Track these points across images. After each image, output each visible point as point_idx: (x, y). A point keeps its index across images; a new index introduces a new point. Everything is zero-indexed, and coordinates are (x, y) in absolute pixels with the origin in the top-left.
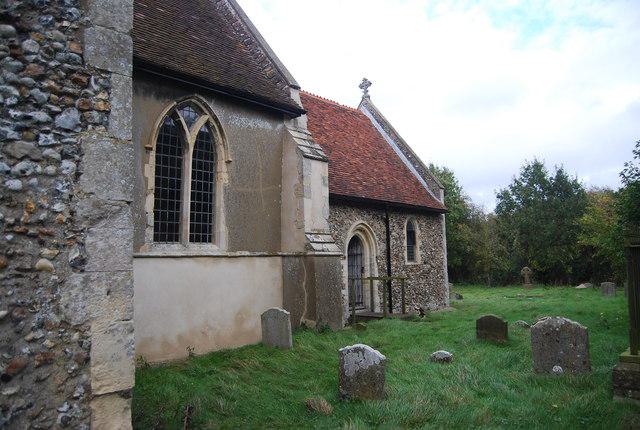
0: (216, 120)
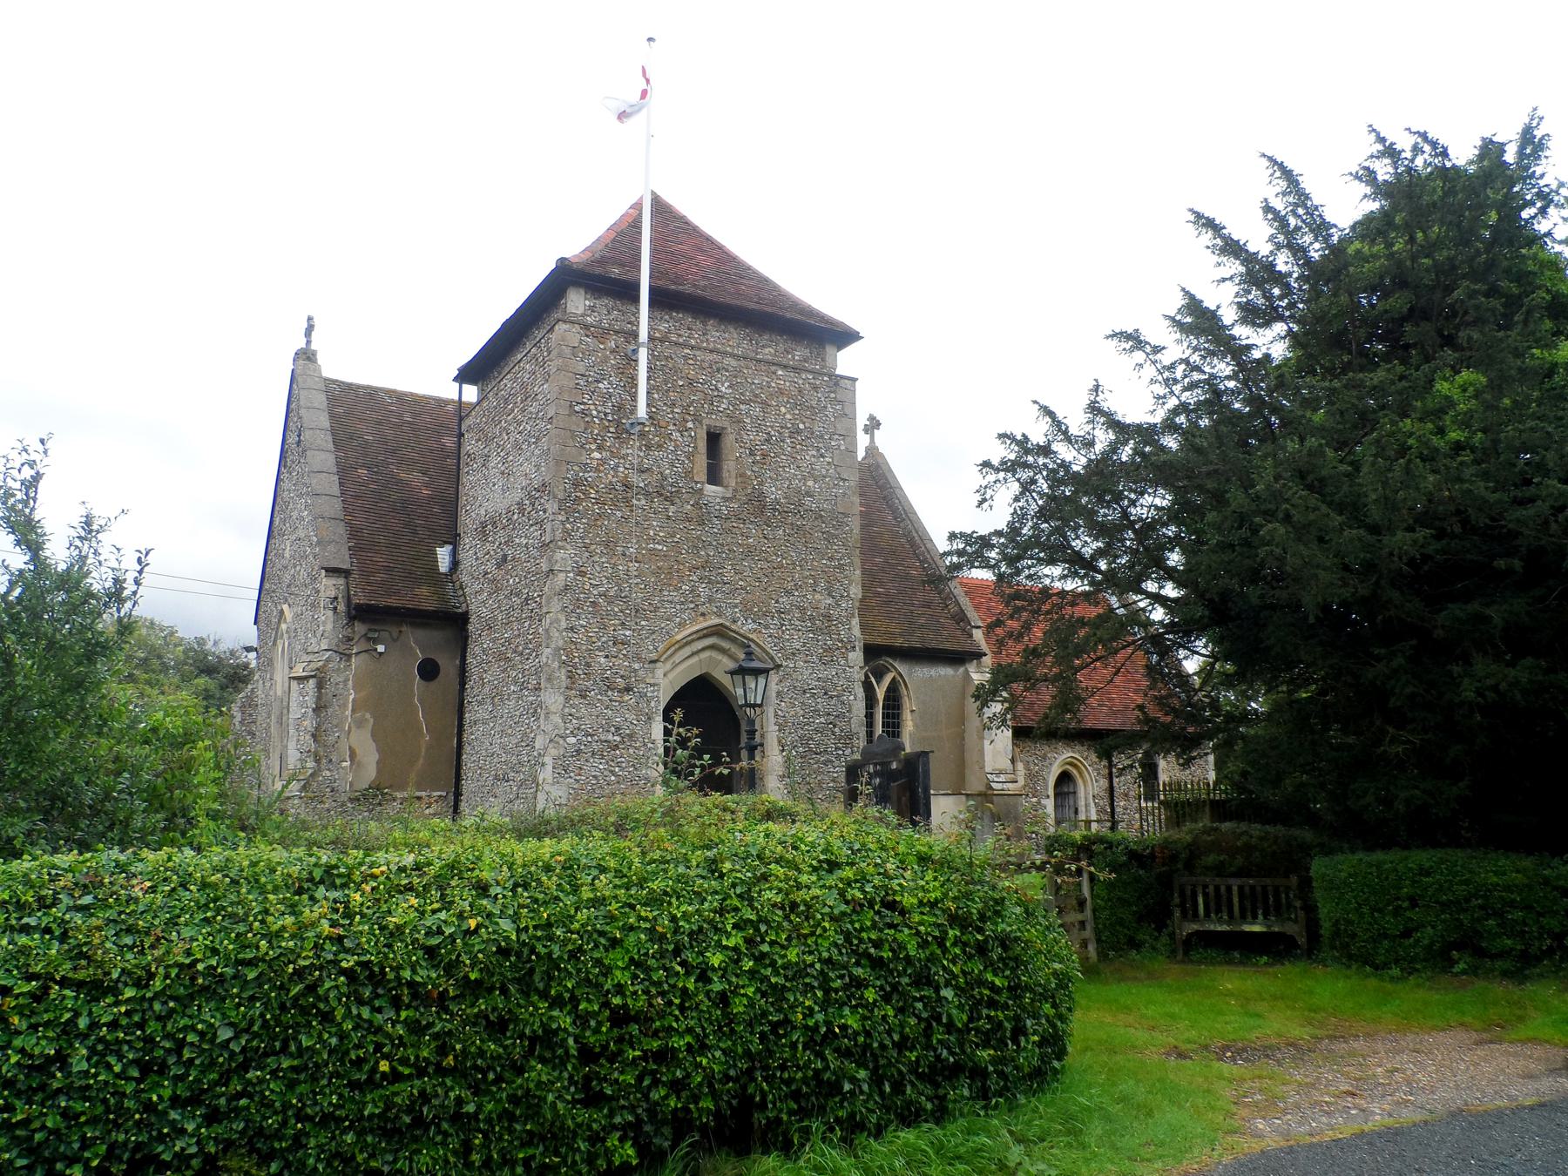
0: (901, 676)
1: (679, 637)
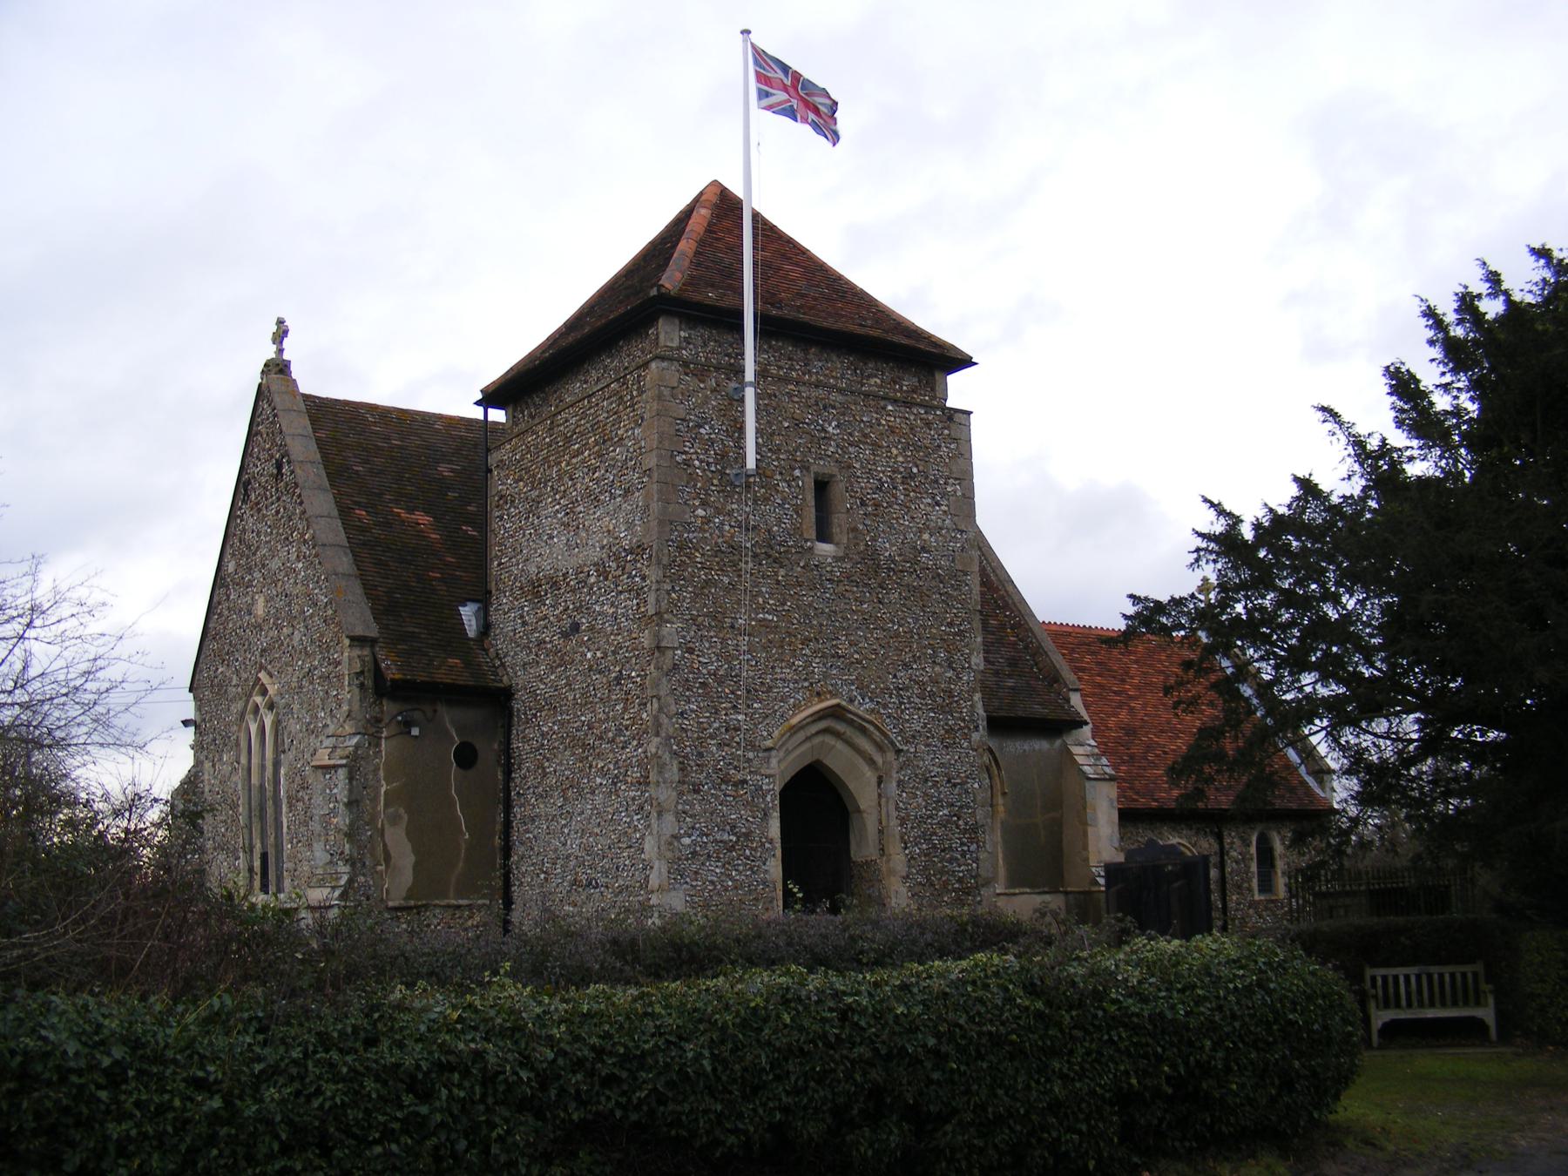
1: (794, 721)
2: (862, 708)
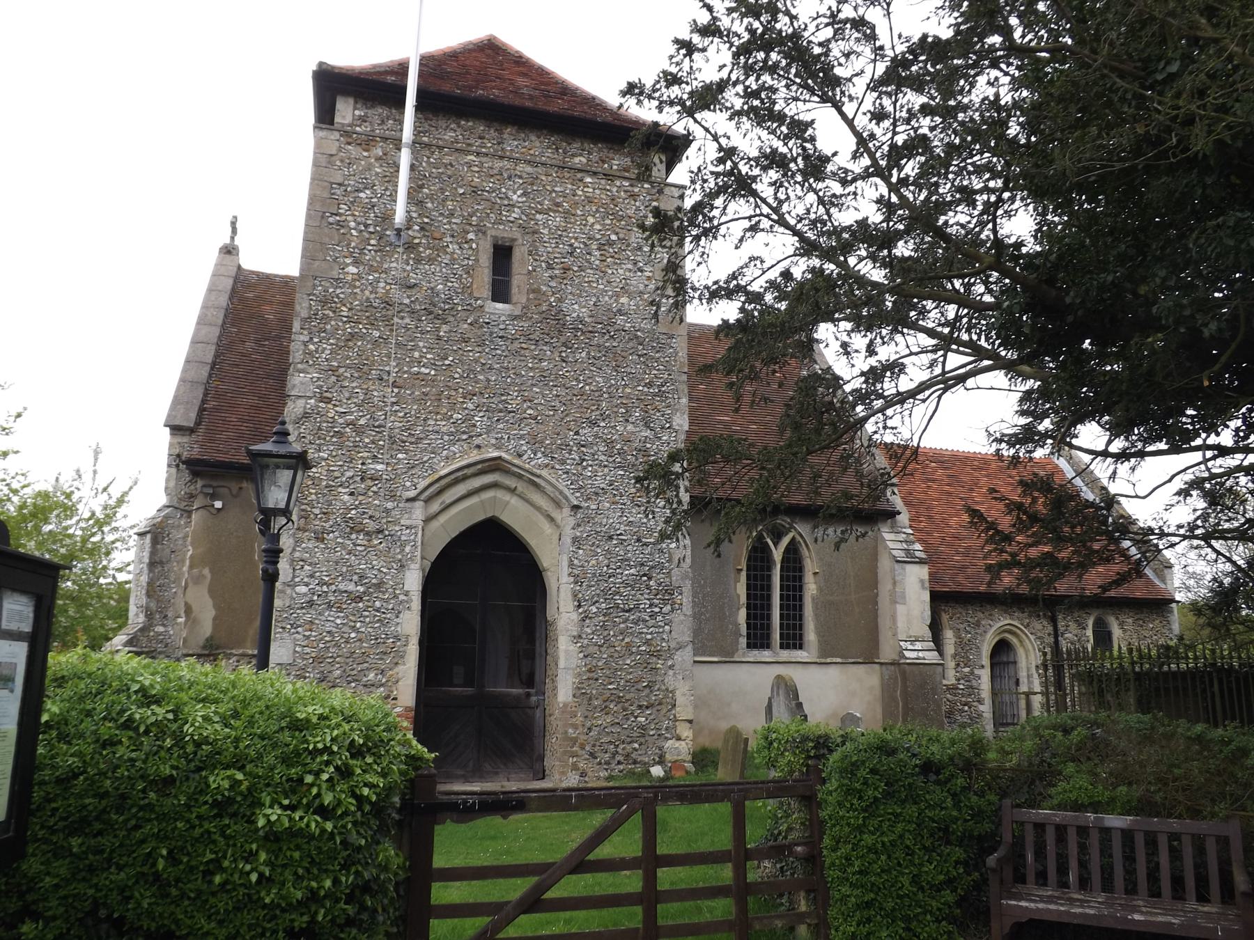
1: (443, 472)
2: (534, 462)
